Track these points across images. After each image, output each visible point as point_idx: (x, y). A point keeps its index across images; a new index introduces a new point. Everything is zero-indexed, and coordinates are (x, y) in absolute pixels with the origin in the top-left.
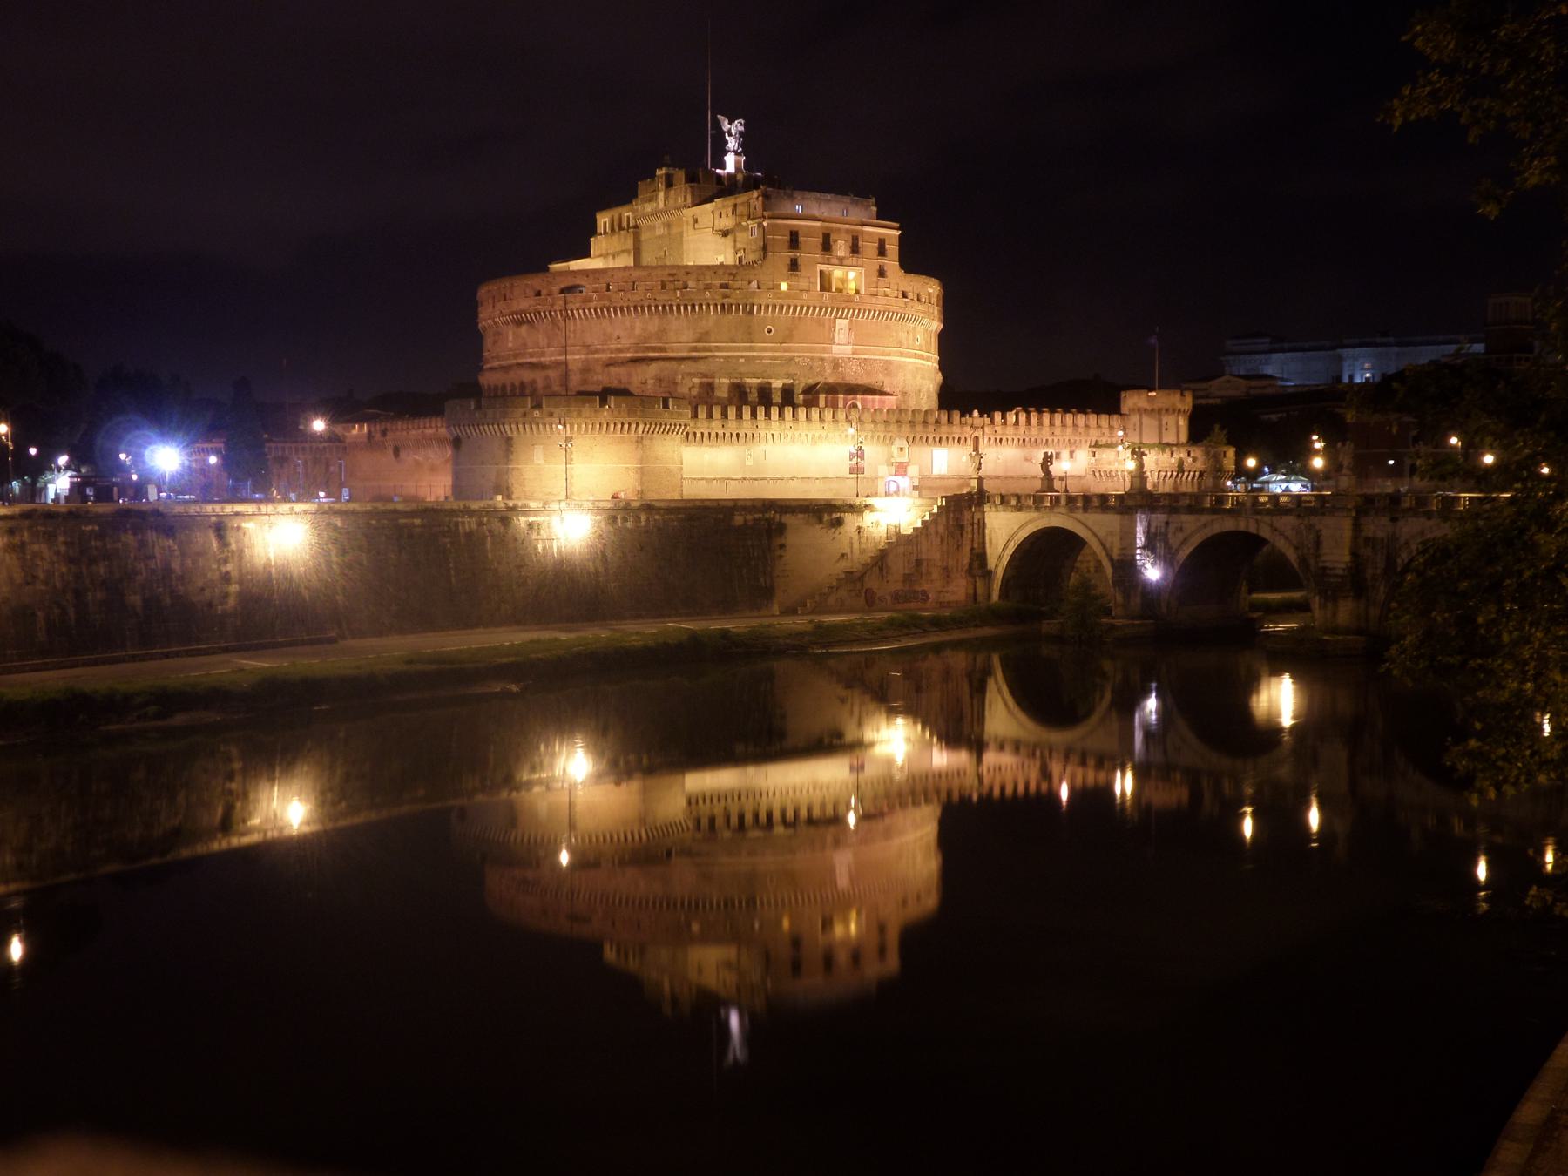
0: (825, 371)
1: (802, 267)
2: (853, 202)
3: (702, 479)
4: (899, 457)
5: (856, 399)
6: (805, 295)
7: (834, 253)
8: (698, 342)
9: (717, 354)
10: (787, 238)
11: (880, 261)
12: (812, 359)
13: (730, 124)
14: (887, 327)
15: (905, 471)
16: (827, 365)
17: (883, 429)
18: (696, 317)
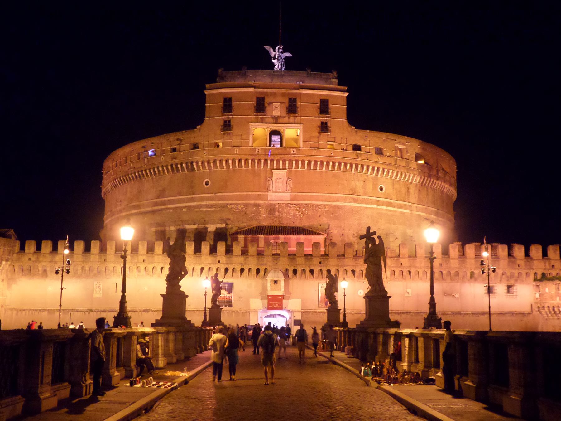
0: (261, 216)
1: (235, 127)
2: (308, 76)
3: (44, 310)
4: (272, 289)
5: (278, 238)
6: (236, 151)
7: (268, 113)
10: (221, 104)
11: (323, 118)
12: (246, 205)
13: (274, 51)
14: (334, 176)
15: (281, 305)
16: (262, 211)
17: (256, 262)
18: (158, 178)
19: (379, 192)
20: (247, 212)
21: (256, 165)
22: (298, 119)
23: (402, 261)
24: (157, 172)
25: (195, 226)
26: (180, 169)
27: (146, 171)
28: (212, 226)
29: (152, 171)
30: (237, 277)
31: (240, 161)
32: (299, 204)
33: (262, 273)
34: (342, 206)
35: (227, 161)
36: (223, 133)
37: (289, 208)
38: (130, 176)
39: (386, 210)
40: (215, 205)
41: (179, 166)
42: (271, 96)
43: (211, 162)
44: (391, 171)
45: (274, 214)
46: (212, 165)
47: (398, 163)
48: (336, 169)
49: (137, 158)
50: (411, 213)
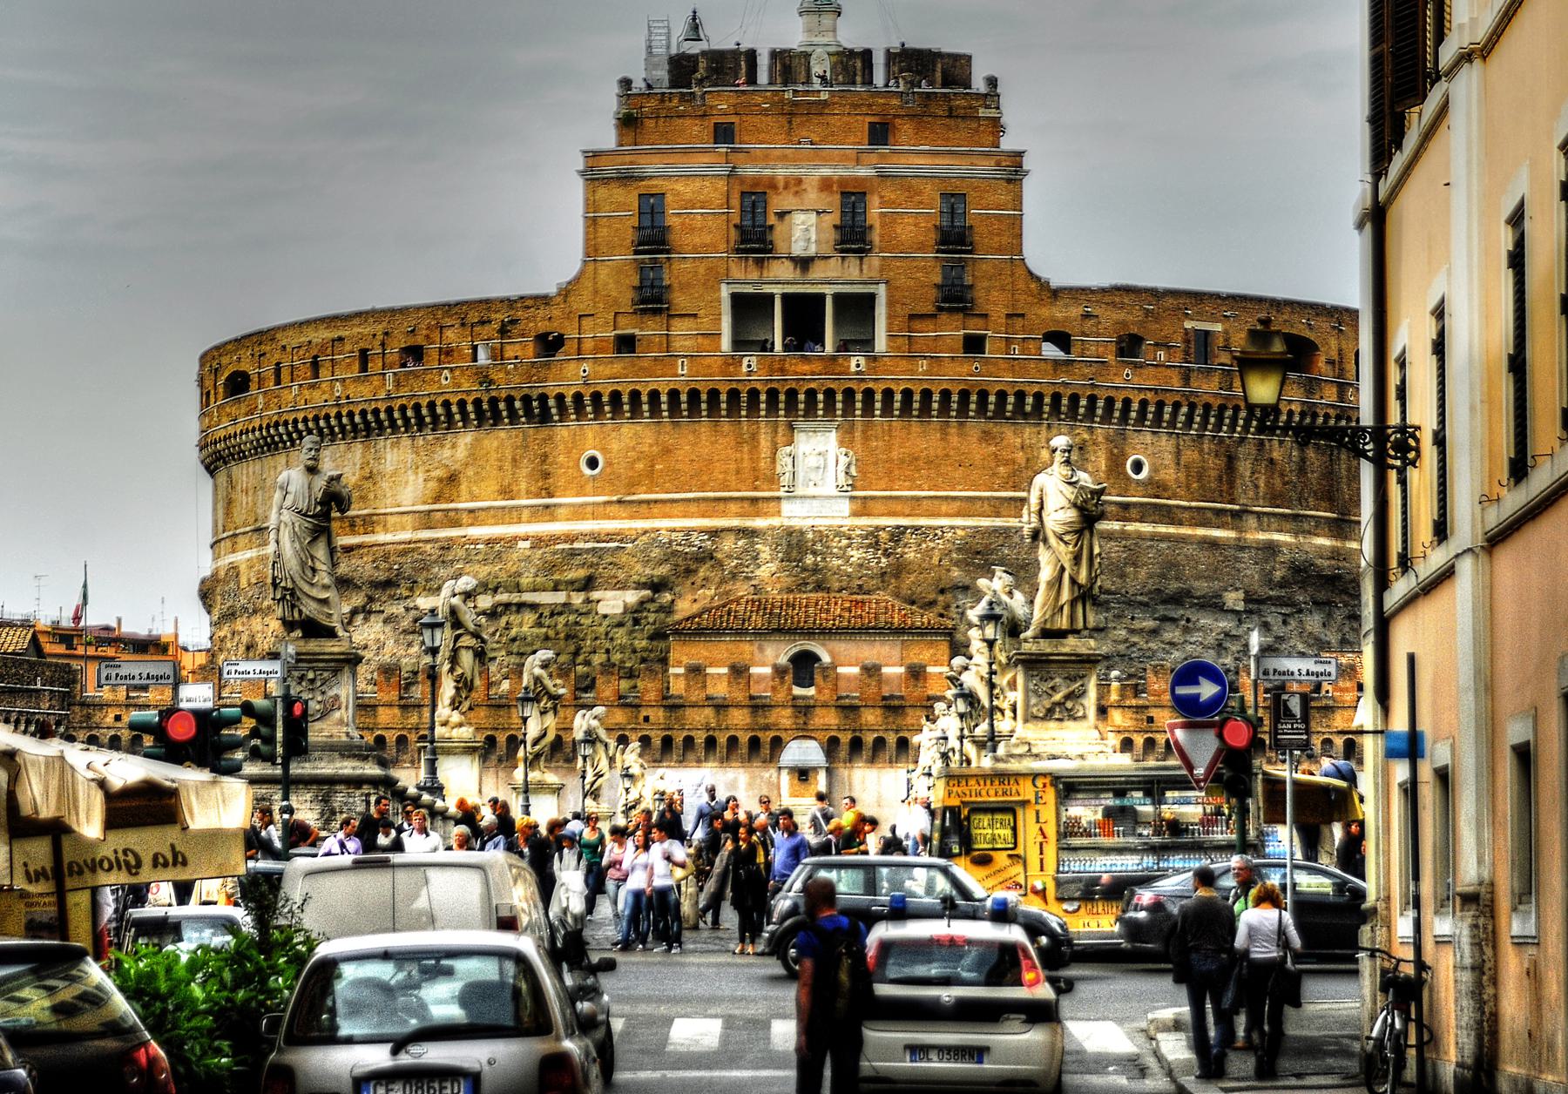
0: (759, 567)
4: (794, 795)
7: (781, 247)
8: (437, 500)
9: (475, 532)
12: (715, 533)
14: (986, 436)
16: (765, 551)
17: (748, 721)
19: (1128, 478)
20: (719, 556)
21: (744, 413)
22: (874, 262)
23: (1153, 713)
24: (428, 420)
25: (560, 597)
26: (505, 414)
27: (389, 410)
28: (610, 594)
29: (410, 413)
30: (699, 761)
31: (694, 395)
32: (878, 529)
33: (766, 750)
34: (1009, 528)
35: (654, 395)
36: (641, 310)
37: (845, 542)
38: (333, 422)
39: (1154, 537)
40: (618, 534)
41: (502, 406)
42: (786, 187)
43: (605, 399)
44: (1168, 409)
45: (800, 561)
46: (607, 408)
47: (1194, 383)
48: (989, 414)
49: (356, 366)
50: (1239, 539)
